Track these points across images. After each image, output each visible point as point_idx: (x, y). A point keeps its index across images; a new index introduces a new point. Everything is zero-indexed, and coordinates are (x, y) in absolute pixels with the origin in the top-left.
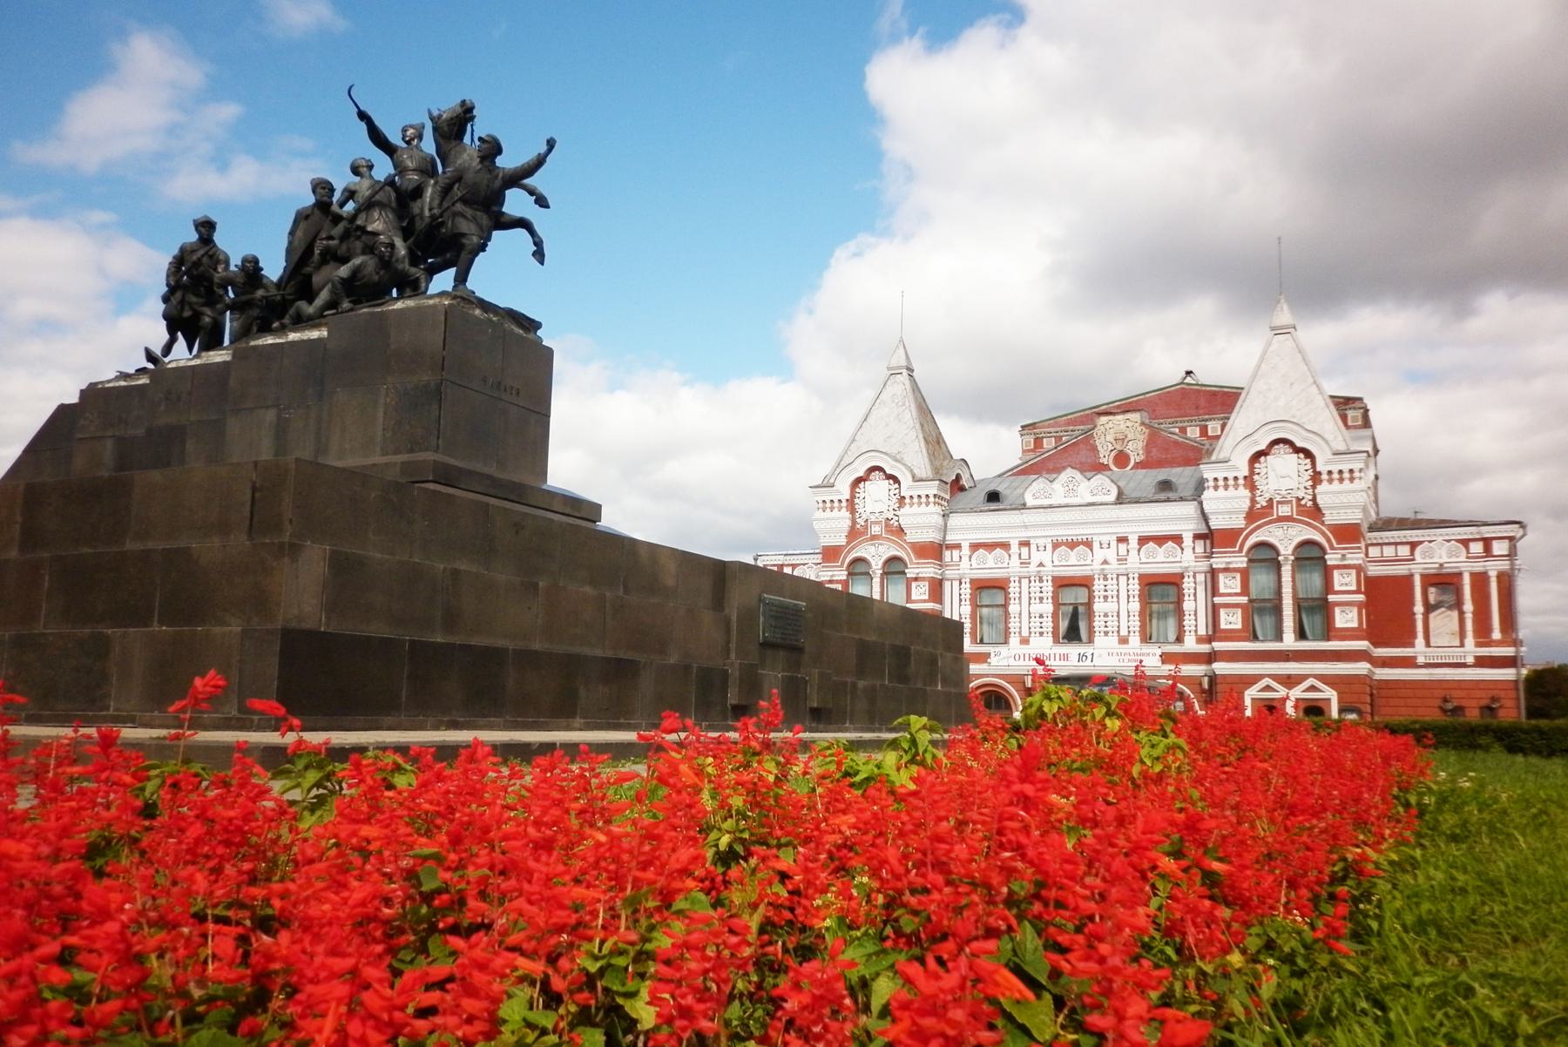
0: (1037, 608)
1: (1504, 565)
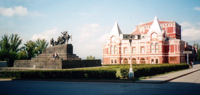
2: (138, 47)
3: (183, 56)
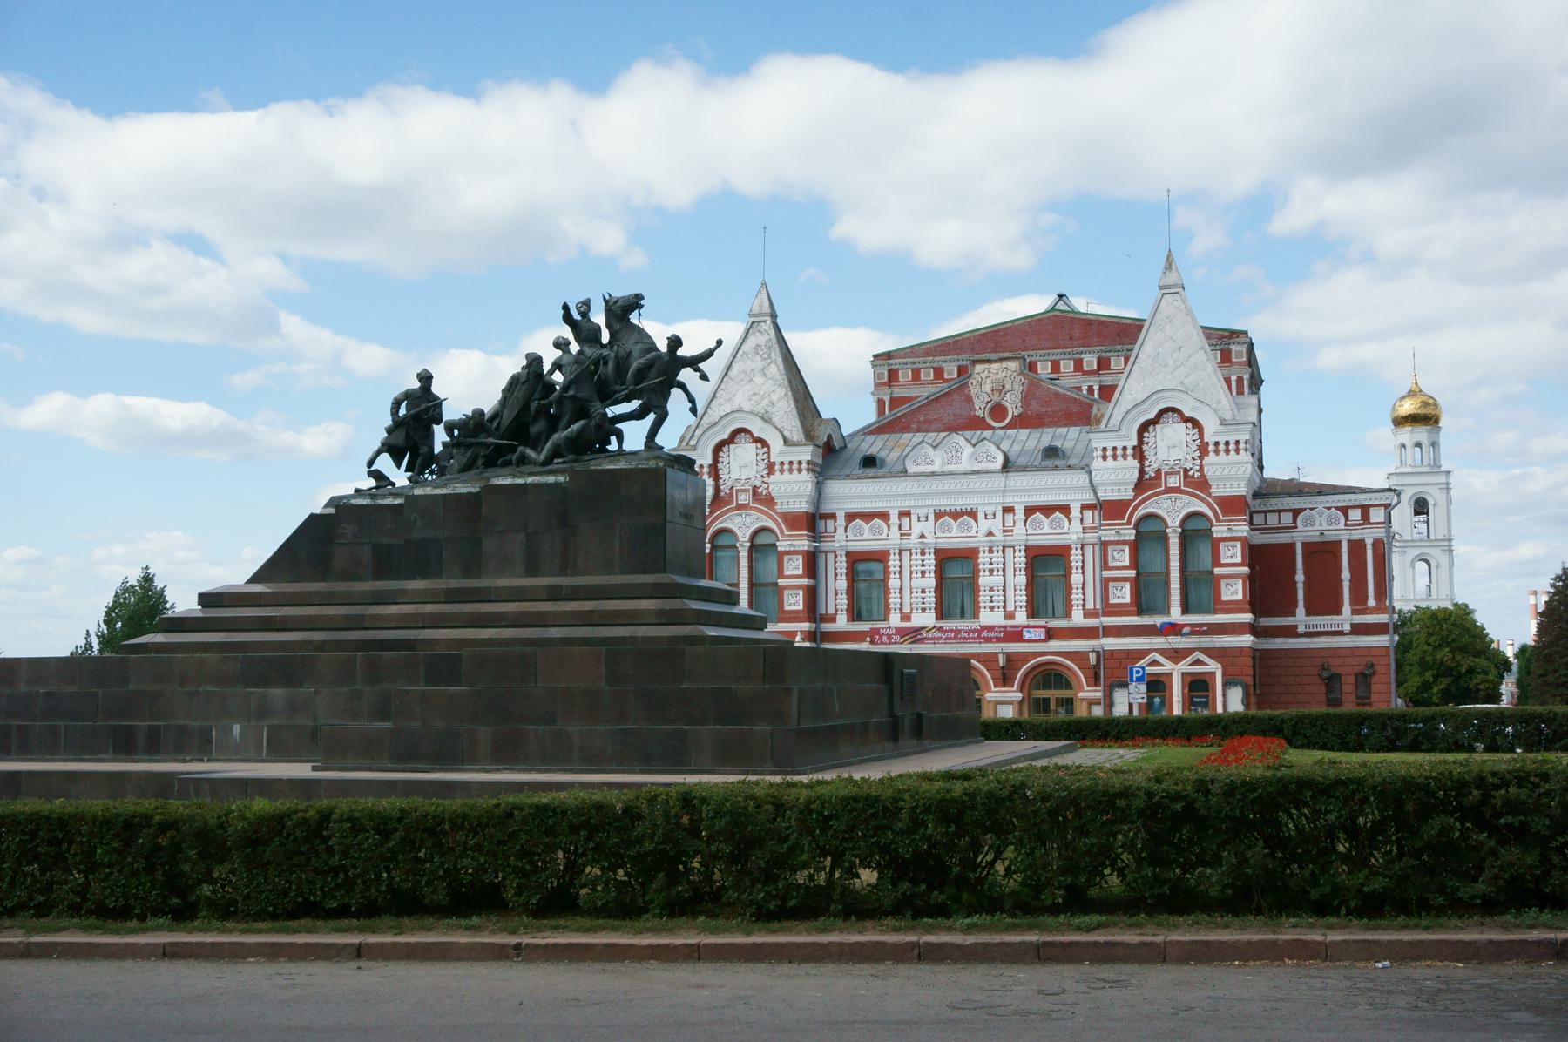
0: (919, 582)
1: (1380, 533)
2: (997, 557)
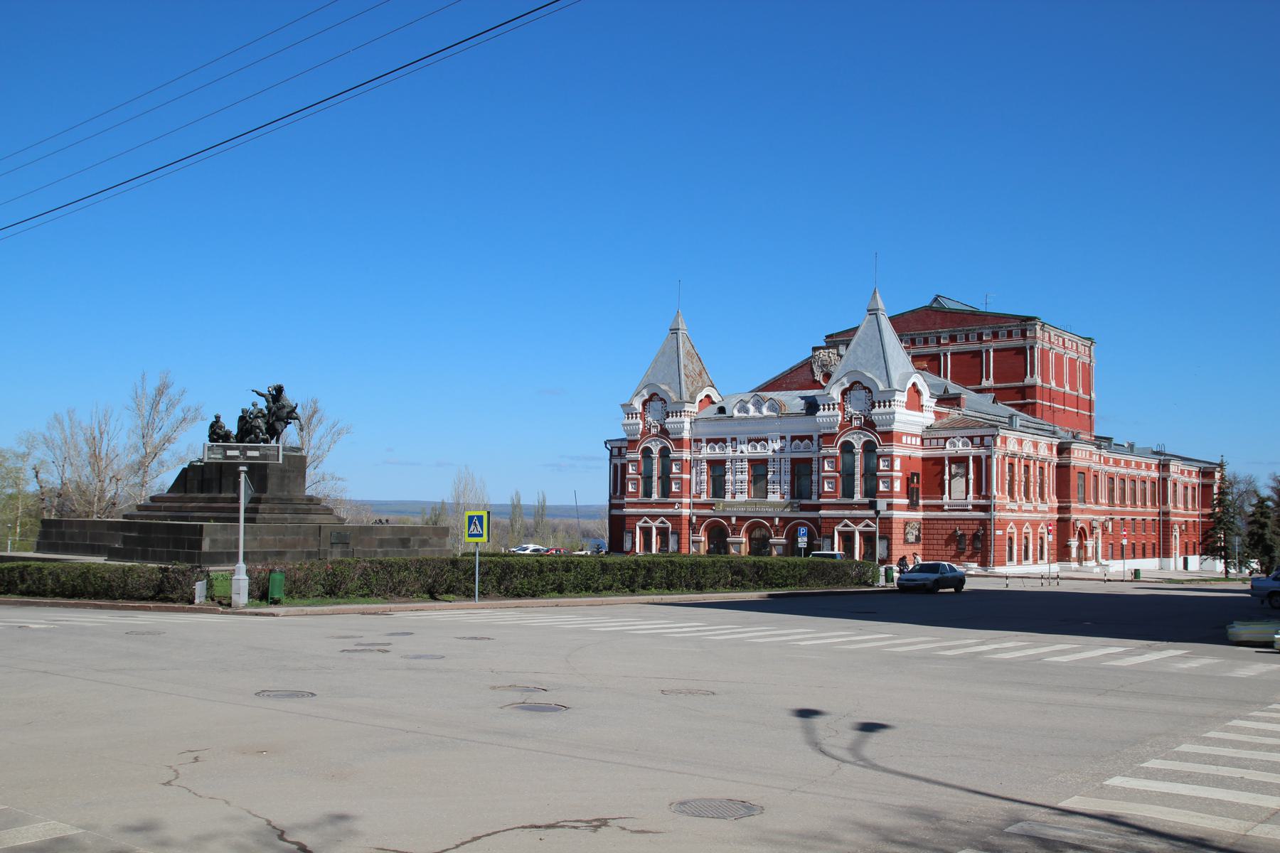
3: (1035, 524)
